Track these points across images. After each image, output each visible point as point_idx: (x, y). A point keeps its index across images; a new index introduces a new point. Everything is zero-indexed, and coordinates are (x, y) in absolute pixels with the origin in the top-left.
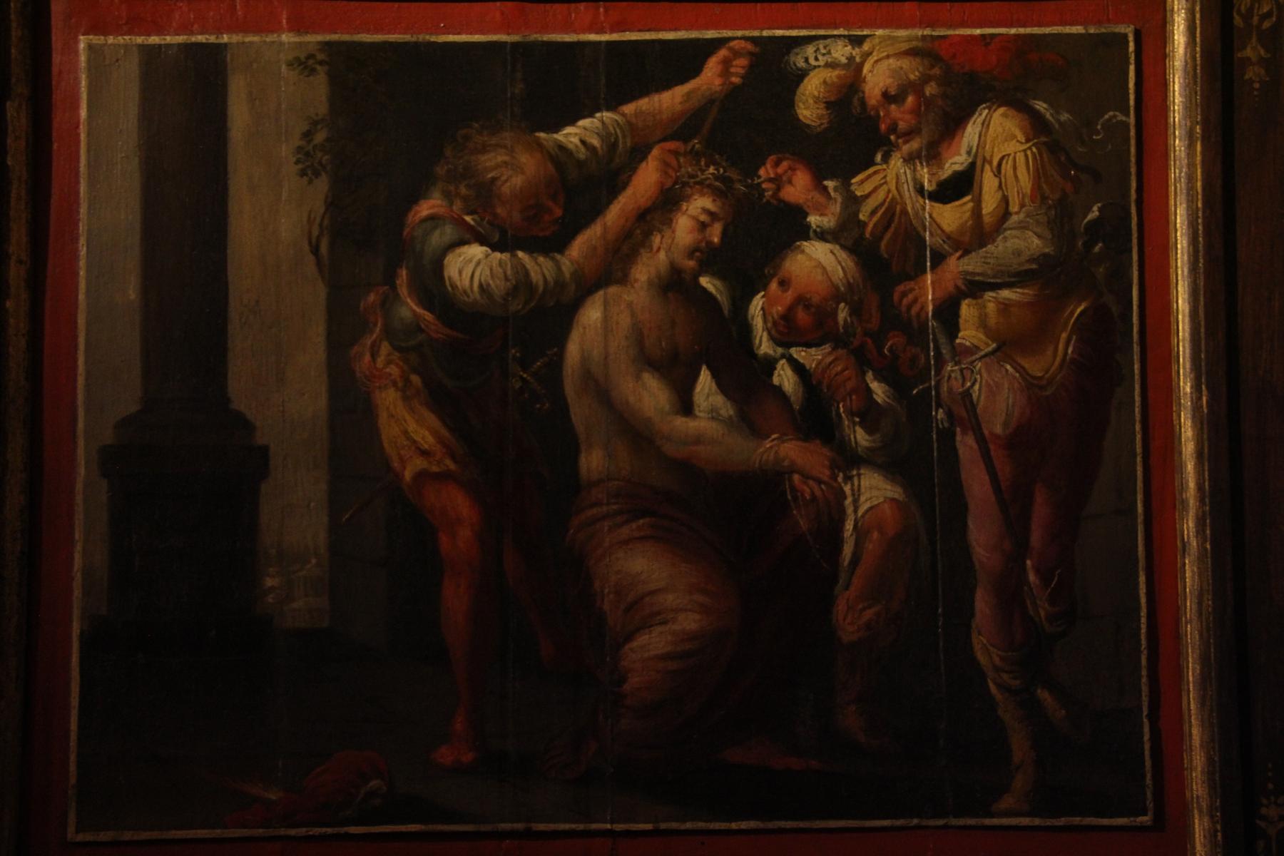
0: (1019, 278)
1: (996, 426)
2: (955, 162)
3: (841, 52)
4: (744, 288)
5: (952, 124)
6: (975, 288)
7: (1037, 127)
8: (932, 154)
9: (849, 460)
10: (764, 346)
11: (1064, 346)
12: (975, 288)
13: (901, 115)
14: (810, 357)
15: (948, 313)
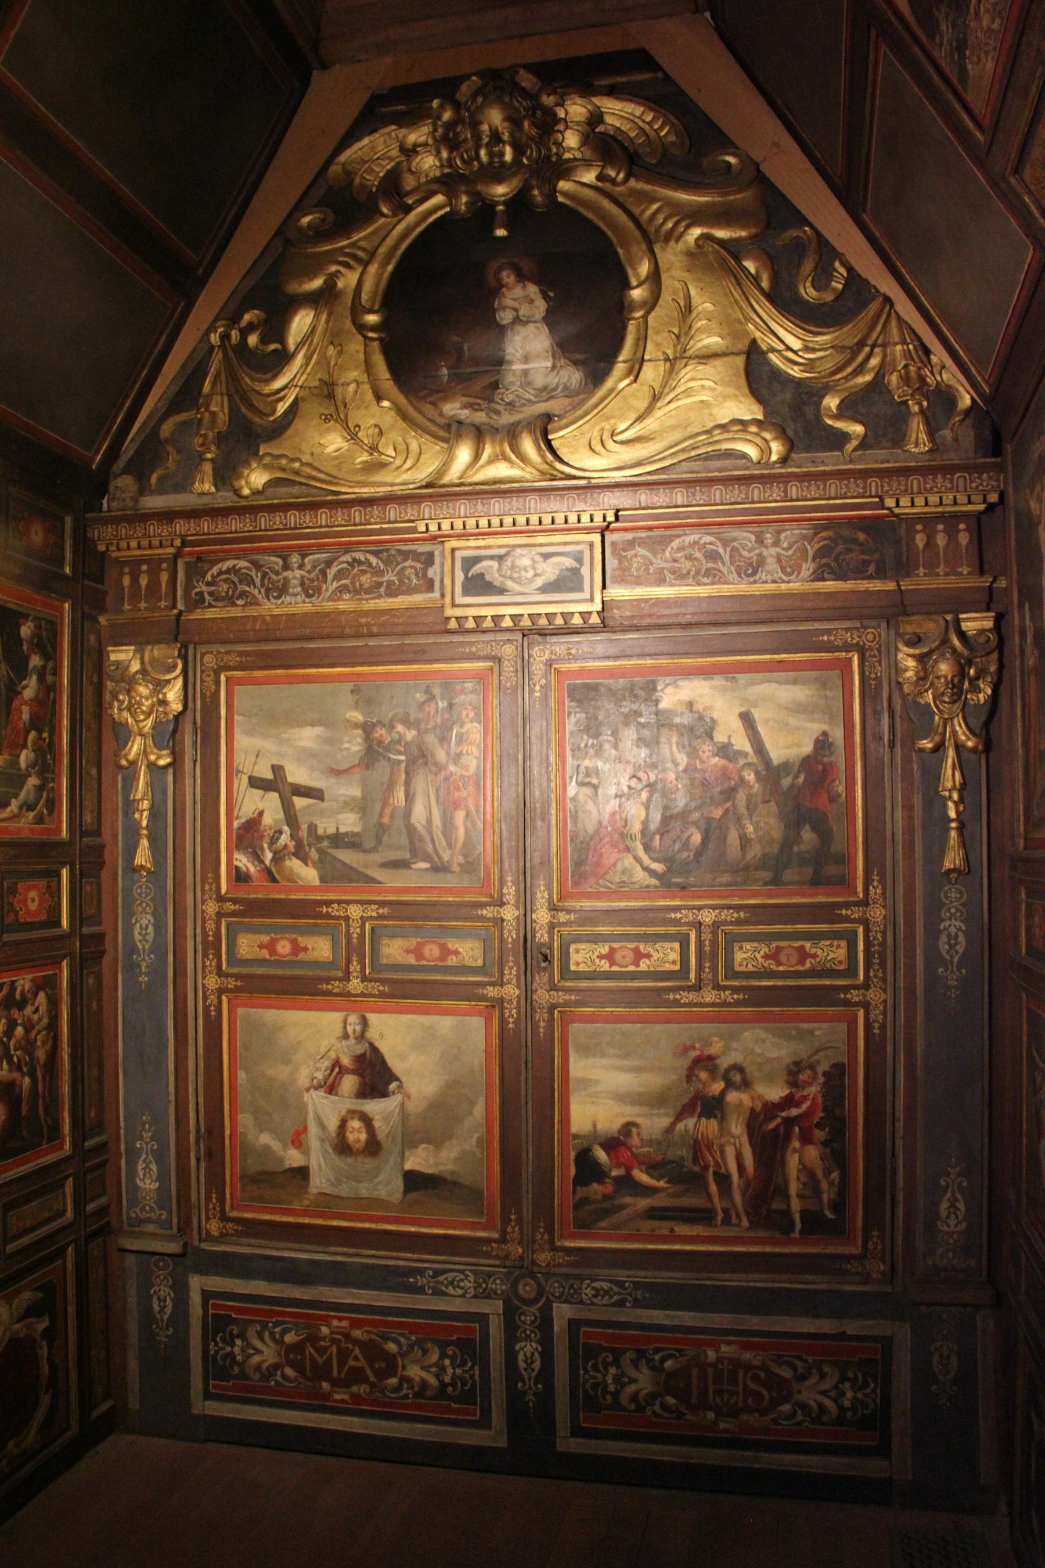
0: (45, 1029)
1: (42, 1062)
2: (36, 1005)
3: (22, 982)
4: (9, 1039)
5: (36, 995)
6: (39, 1032)
7: (47, 995)
8: (33, 1004)
9: (23, 1076)
10: (12, 1052)
11: (50, 1043)
12: (39, 1032)
13: (29, 995)
14: (18, 1053)
15: (36, 1039)
